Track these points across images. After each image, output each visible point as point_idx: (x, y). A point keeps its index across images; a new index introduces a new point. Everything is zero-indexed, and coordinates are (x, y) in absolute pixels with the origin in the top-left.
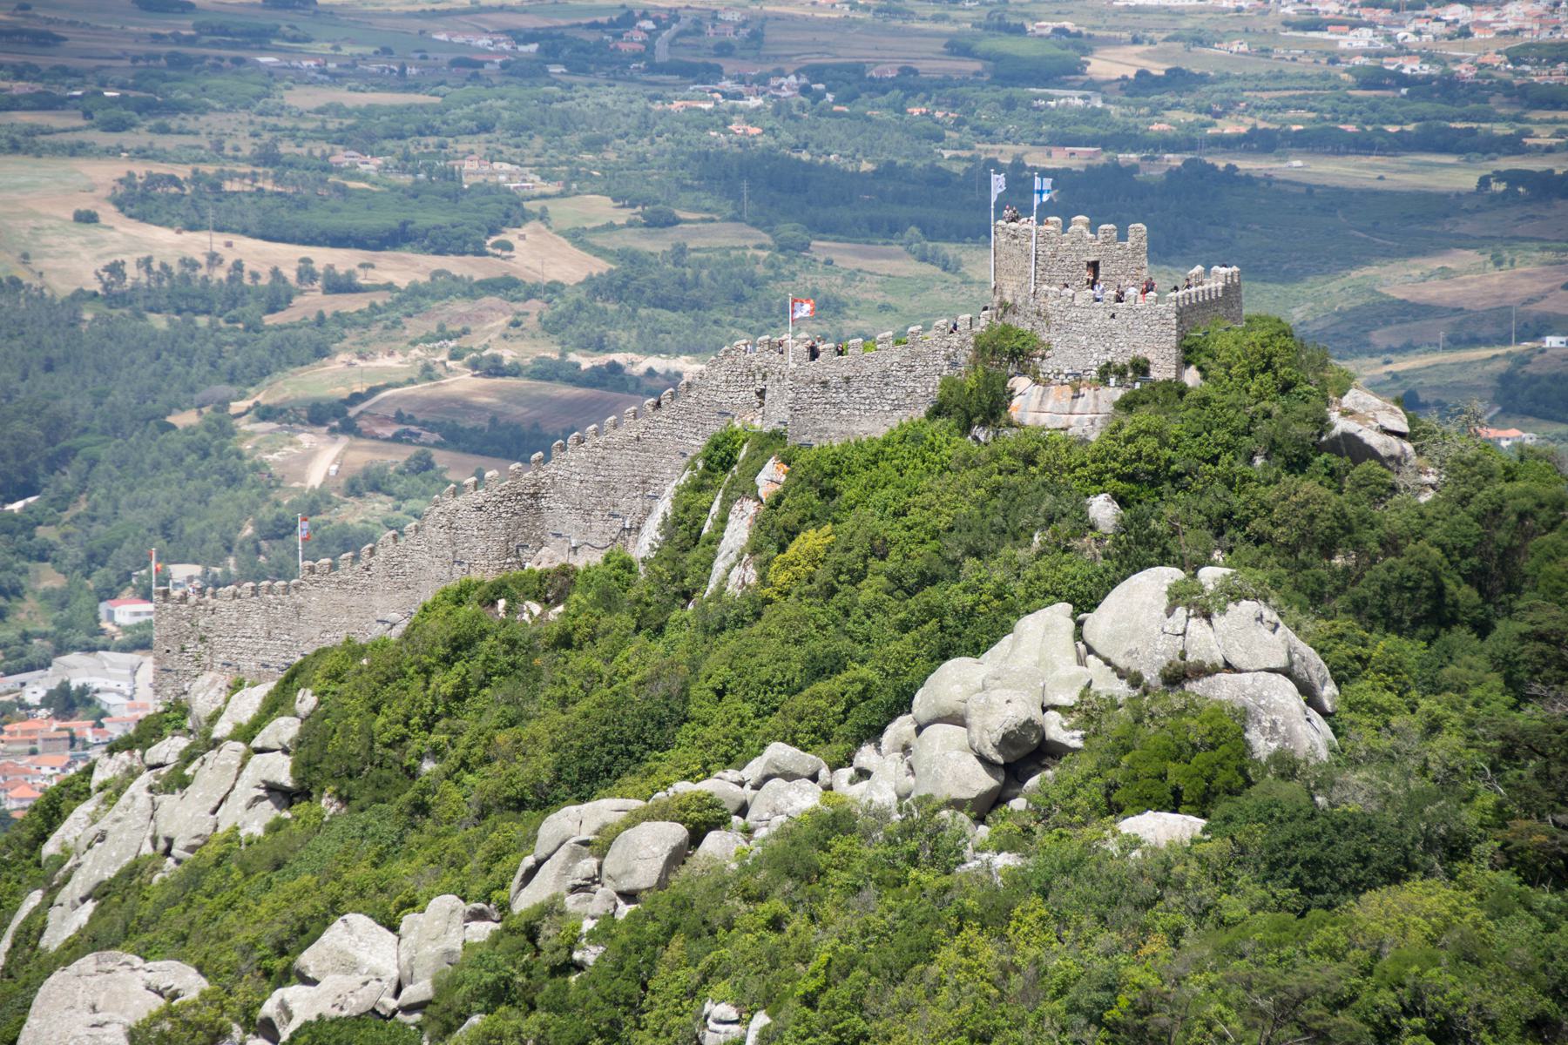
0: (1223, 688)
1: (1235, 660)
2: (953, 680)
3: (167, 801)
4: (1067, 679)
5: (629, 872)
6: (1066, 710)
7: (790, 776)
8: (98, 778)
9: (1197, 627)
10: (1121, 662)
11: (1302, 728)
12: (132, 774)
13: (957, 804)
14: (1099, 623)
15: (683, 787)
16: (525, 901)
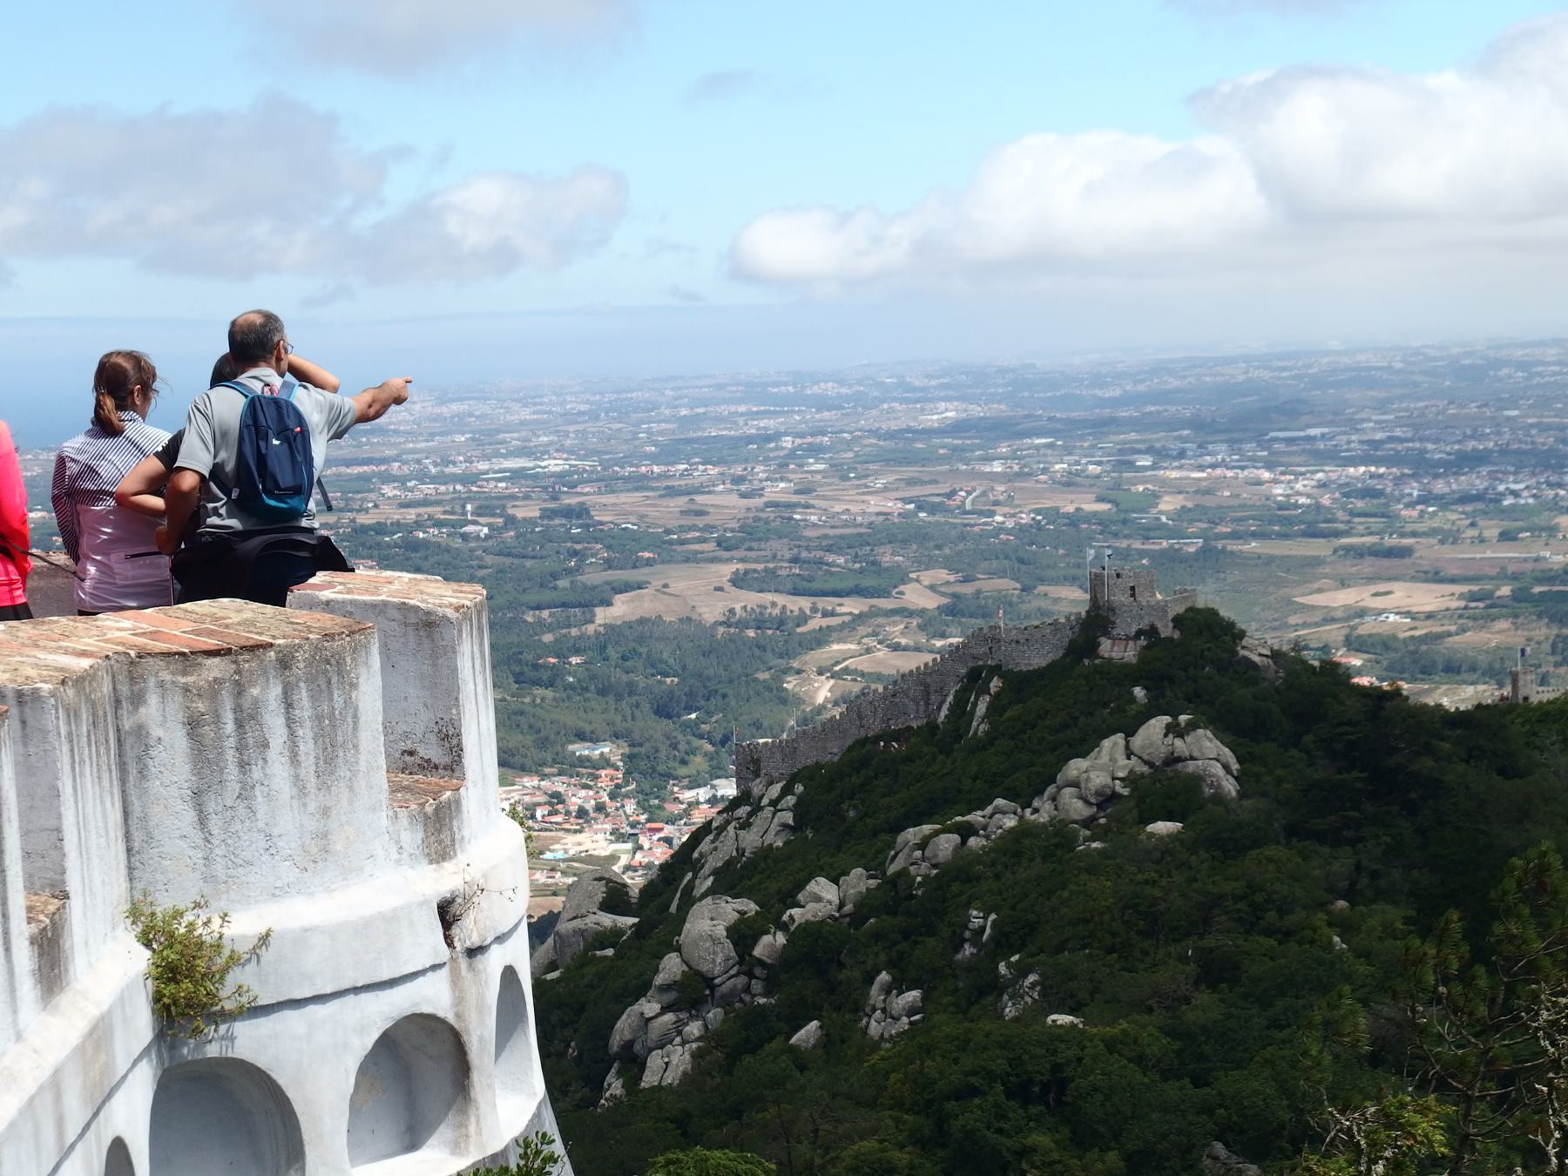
0: (1191, 766)
1: (1195, 754)
2: (1076, 767)
3: (741, 833)
4: (1123, 766)
5: (936, 856)
7: (1005, 813)
8: (715, 824)
9: (1178, 742)
10: (1146, 757)
11: (1224, 783)
12: (728, 823)
13: (1075, 822)
14: (1138, 741)
15: (959, 818)
16: (892, 869)
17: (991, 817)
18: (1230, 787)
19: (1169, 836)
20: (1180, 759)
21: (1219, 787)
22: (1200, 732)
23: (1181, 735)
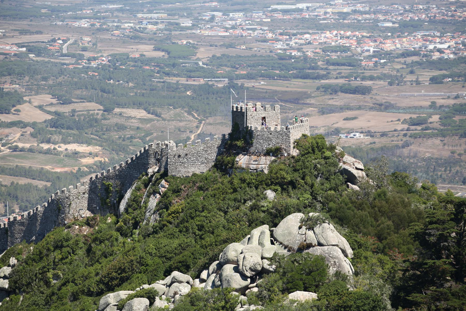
0: (318, 251)
1: (322, 241)
2: (233, 250)
4: (270, 250)
6: (270, 259)
7: (180, 282)
9: (310, 233)
10: (286, 243)
11: (344, 263)
13: (236, 290)
14: (279, 231)
15: (146, 286)
17: (170, 286)
18: (347, 268)
19: (307, 302)
20: (309, 246)
21: (340, 266)
22: (326, 225)
23: (311, 228)
